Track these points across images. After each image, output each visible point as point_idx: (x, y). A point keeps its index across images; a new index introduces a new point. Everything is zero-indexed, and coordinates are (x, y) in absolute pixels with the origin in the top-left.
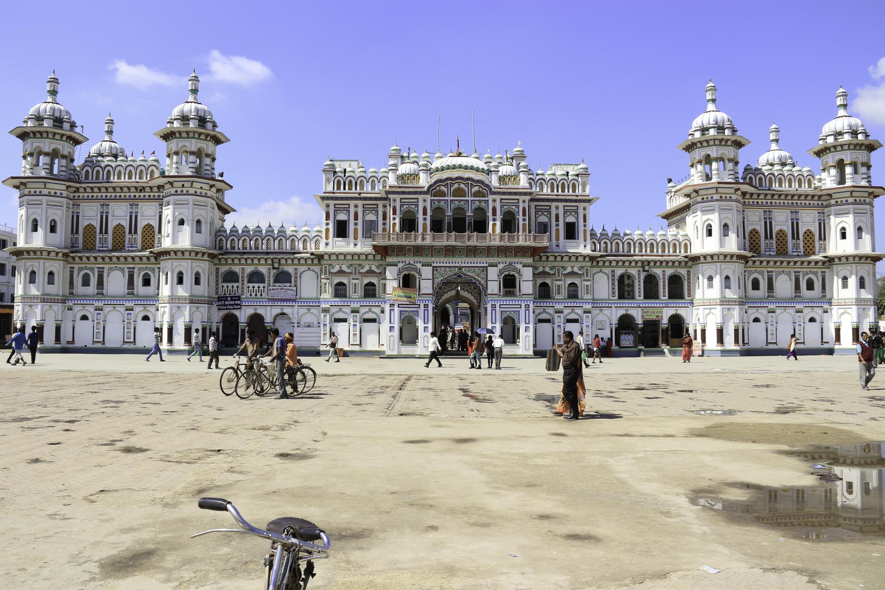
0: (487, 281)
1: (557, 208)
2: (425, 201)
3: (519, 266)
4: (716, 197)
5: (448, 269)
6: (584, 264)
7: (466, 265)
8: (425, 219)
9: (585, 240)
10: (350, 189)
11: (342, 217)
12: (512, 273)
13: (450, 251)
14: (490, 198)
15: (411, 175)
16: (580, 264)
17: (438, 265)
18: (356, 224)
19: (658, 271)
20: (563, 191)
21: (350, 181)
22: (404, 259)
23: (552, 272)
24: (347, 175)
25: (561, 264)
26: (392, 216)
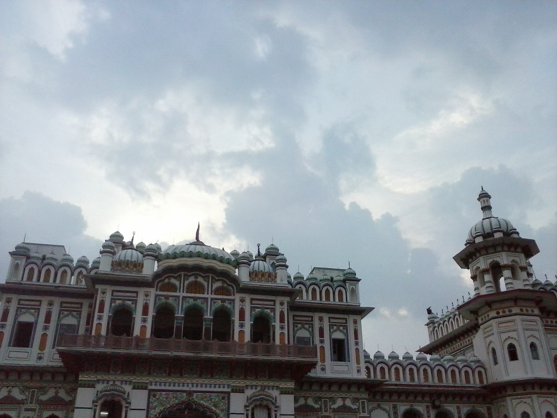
0: (229, 414)
1: (321, 319)
2: (147, 295)
3: (275, 393)
4: (516, 310)
5: (171, 395)
6: (358, 396)
7: (199, 389)
8: (144, 321)
9: (358, 362)
10: (46, 280)
11: (26, 318)
12: (265, 403)
13: (176, 367)
14: (237, 297)
15: (131, 262)
16: (354, 395)
17: (158, 387)
18: (46, 328)
19: (451, 408)
20: (328, 298)
21: (48, 271)
22: (106, 377)
23: (317, 406)
24: (45, 262)
25: (328, 395)
26: (96, 314)
